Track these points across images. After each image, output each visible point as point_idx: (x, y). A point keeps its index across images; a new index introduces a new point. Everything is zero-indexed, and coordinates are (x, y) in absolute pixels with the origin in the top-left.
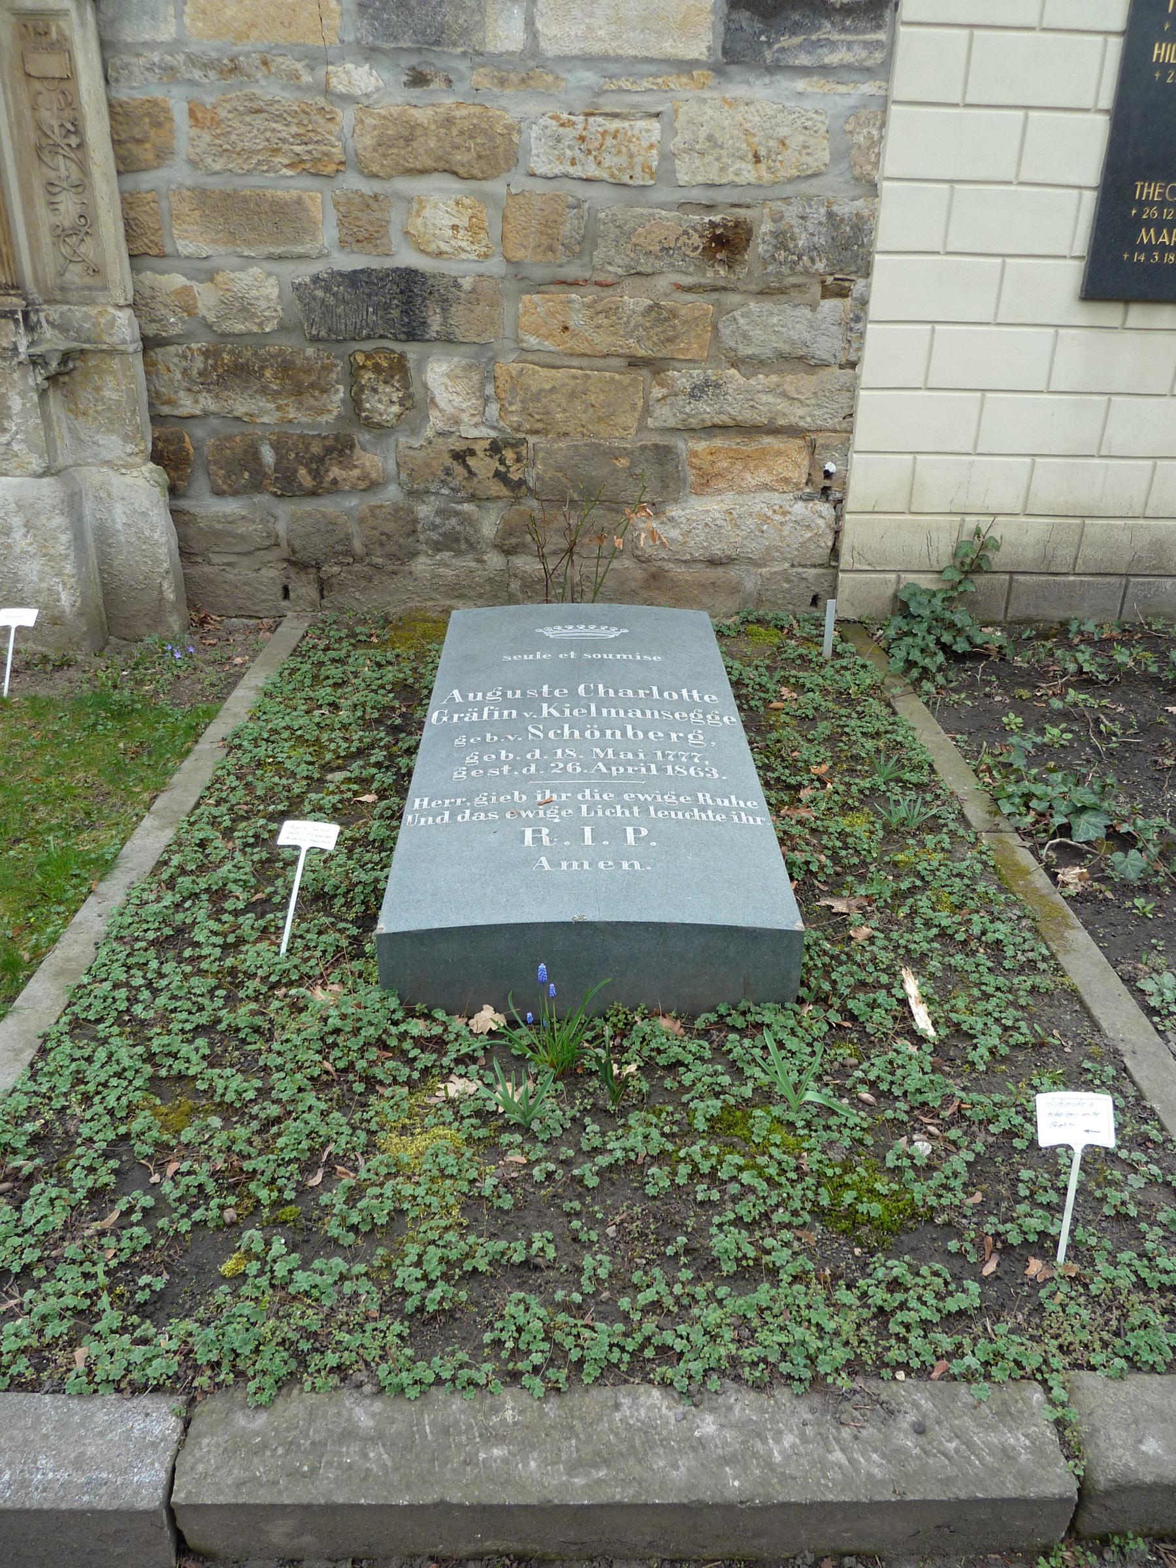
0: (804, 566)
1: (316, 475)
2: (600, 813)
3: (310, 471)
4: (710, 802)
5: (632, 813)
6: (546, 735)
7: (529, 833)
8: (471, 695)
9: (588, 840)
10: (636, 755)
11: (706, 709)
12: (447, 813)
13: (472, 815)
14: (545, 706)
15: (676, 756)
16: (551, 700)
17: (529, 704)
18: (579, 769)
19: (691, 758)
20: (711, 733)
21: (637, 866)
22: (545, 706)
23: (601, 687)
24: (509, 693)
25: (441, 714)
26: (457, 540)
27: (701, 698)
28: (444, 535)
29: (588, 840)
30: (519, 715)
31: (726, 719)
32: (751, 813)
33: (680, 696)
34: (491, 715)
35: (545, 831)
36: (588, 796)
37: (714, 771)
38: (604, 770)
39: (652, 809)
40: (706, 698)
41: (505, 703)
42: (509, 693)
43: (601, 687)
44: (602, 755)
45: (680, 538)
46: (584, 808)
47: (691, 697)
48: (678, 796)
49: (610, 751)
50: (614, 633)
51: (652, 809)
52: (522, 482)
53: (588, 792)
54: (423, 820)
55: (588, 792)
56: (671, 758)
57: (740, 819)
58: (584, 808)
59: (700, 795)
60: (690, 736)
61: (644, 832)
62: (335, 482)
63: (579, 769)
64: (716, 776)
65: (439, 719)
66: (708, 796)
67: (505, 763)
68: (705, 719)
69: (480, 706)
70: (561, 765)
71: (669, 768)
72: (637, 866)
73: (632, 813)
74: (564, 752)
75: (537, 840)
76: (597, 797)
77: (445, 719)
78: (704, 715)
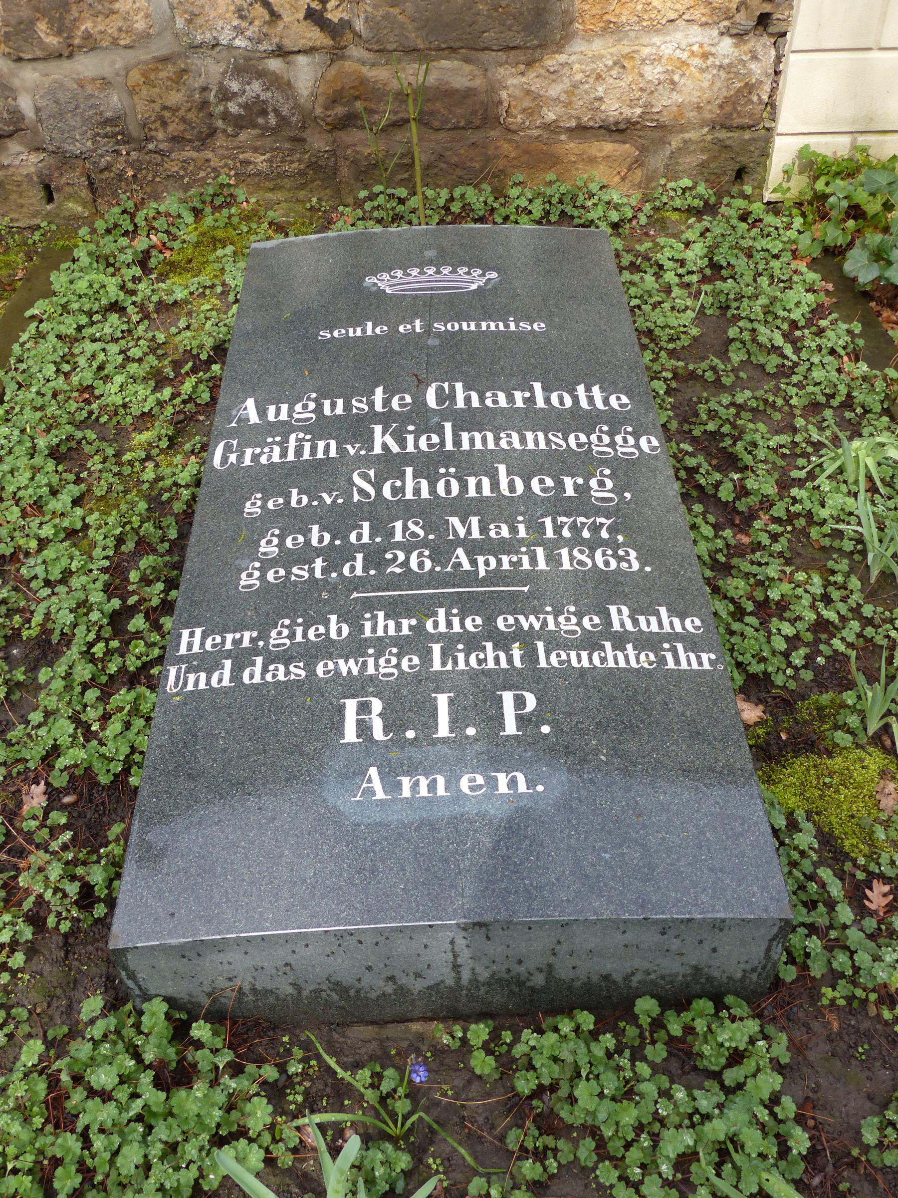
0: (729, 129)
1: (61, 27)
2: (462, 666)
3: (51, 23)
4: (629, 626)
5: (510, 659)
6: (379, 491)
7: (351, 706)
8: (272, 409)
9: (443, 730)
10: (514, 530)
11: (615, 421)
12: (228, 663)
13: (265, 670)
14: (378, 429)
15: (574, 527)
16: (387, 418)
17: (356, 428)
18: (428, 564)
19: (595, 529)
20: (625, 470)
21: (522, 787)
22: (378, 429)
23: (459, 386)
24: (327, 404)
25: (228, 449)
26: (264, 113)
27: (606, 401)
28: (245, 106)
29: (443, 730)
30: (341, 450)
31: (643, 441)
32: (693, 644)
33: (576, 399)
34: (299, 451)
35: (377, 705)
36: (442, 628)
37: (633, 554)
38: (466, 566)
39: (540, 645)
40: (613, 399)
41: (321, 427)
42: (327, 404)
43: (459, 386)
44: (462, 532)
45: (563, 97)
46: (436, 648)
47: (591, 399)
48: (580, 615)
49: (474, 521)
50: (474, 280)
51: (540, 645)
52: (346, 25)
53: (442, 612)
54: (192, 677)
55: (442, 612)
56: (566, 533)
57: (677, 662)
58: (436, 648)
59: (613, 609)
60: (593, 483)
61: (531, 702)
62: (88, 36)
63: (428, 564)
64: (636, 566)
65: (224, 459)
66: (625, 610)
67: (318, 552)
68: (612, 444)
69: (284, 429)
70: (401, 556)
71: (565, 552)
72: (522, 787)
73: (510, 659)
74: (405, 528)
75: (364, 728)
76: (457, 628)
77: (233, 458)
78: (612, 434)
